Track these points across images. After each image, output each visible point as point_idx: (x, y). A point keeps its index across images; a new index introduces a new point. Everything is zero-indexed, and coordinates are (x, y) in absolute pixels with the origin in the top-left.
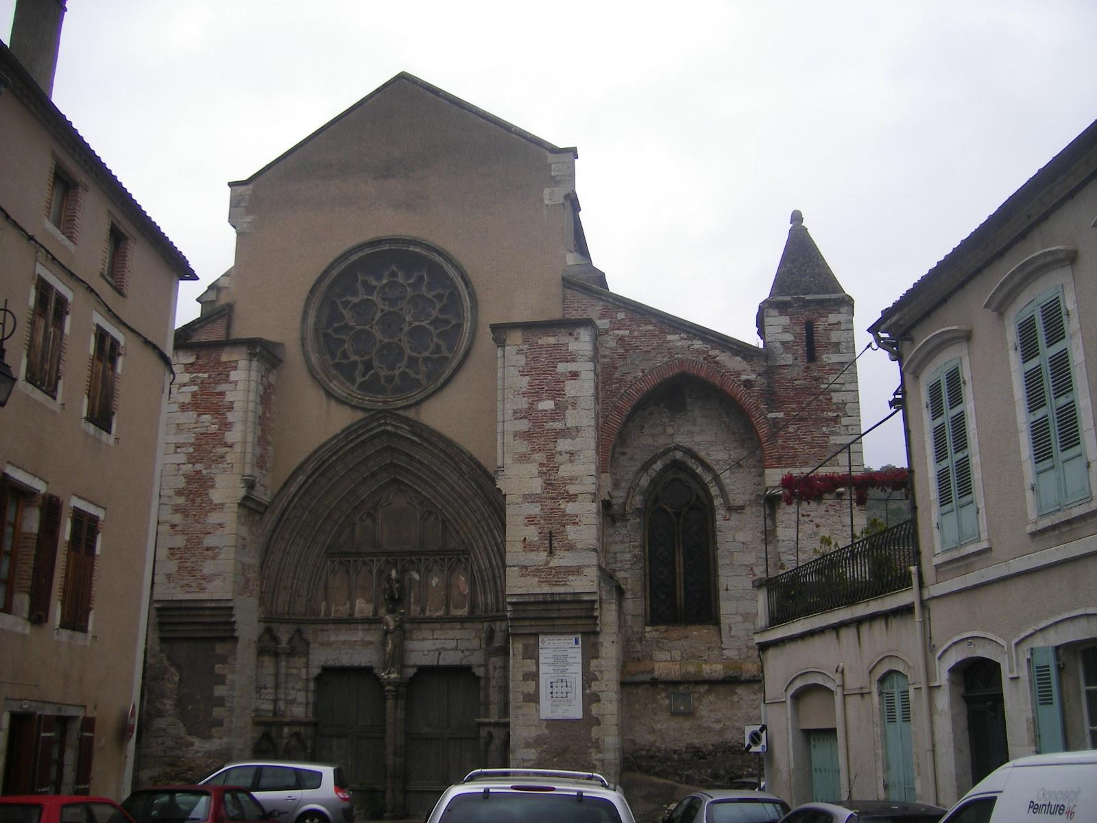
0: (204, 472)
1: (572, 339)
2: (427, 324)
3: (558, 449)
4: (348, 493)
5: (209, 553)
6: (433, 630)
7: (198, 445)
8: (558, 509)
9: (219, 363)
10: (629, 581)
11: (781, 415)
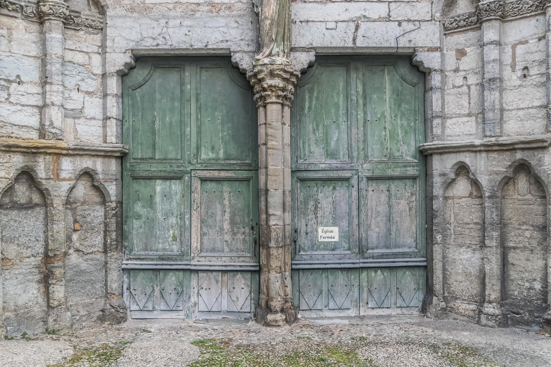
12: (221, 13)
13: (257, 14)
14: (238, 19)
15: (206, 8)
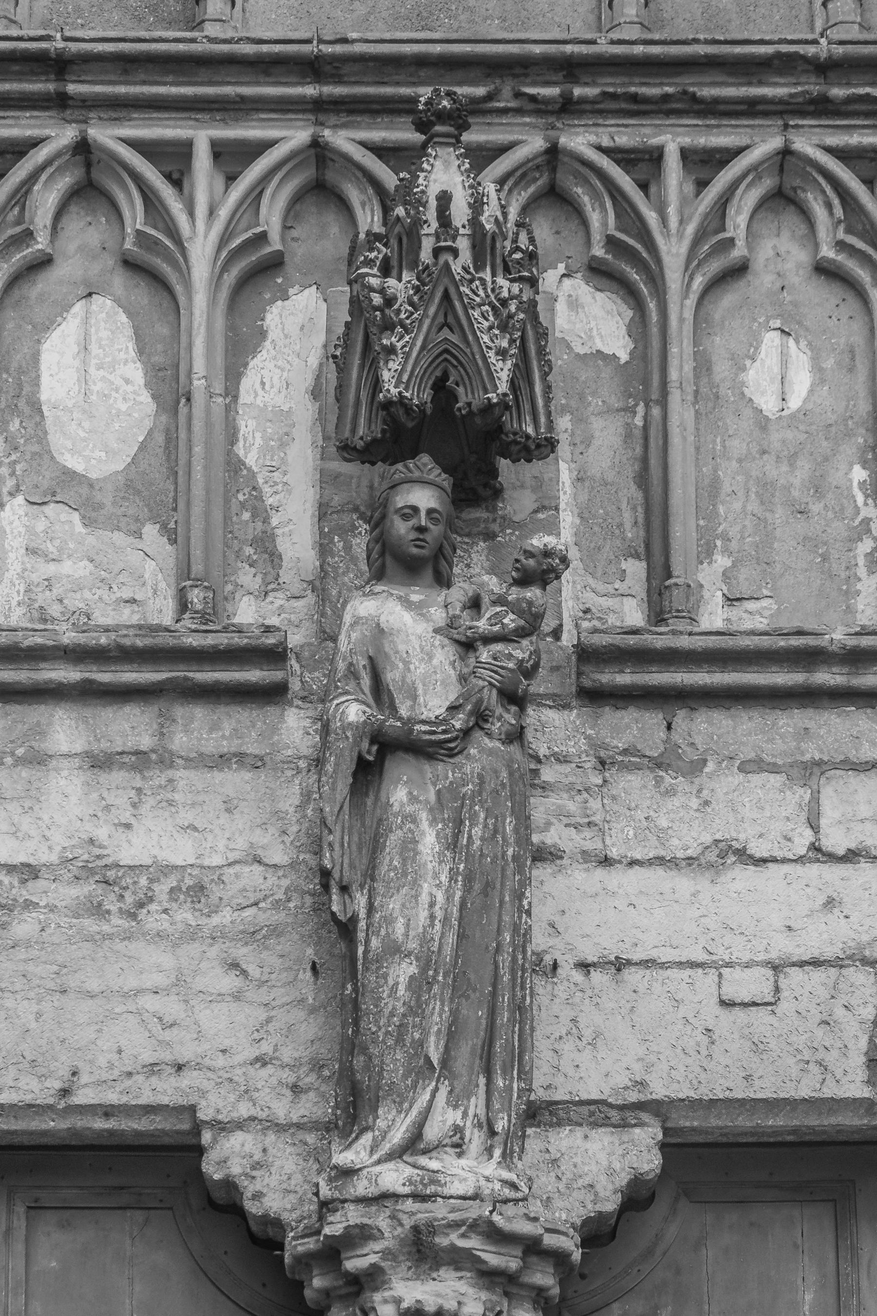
6: (810, 771)
12: (153, 919)
13: (346, 929)
14: (241, 952)
15: (69, 893)
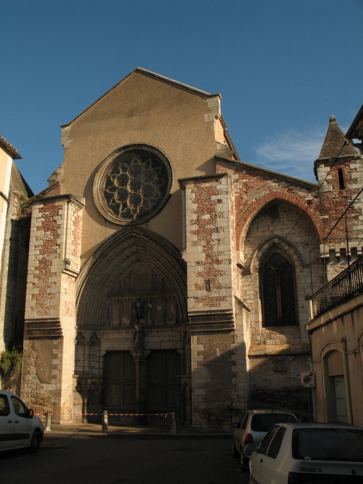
0: (47, 258)
1: (217, 183)
2: (152, 183)
3: (212, 238)
4: (117, 266)
5: (49, 296)
6: (158, 332)
7: (44, 245)
8: (213, 268)
9: (53, 207)
10: (253, 305)
11: (326, 217)
